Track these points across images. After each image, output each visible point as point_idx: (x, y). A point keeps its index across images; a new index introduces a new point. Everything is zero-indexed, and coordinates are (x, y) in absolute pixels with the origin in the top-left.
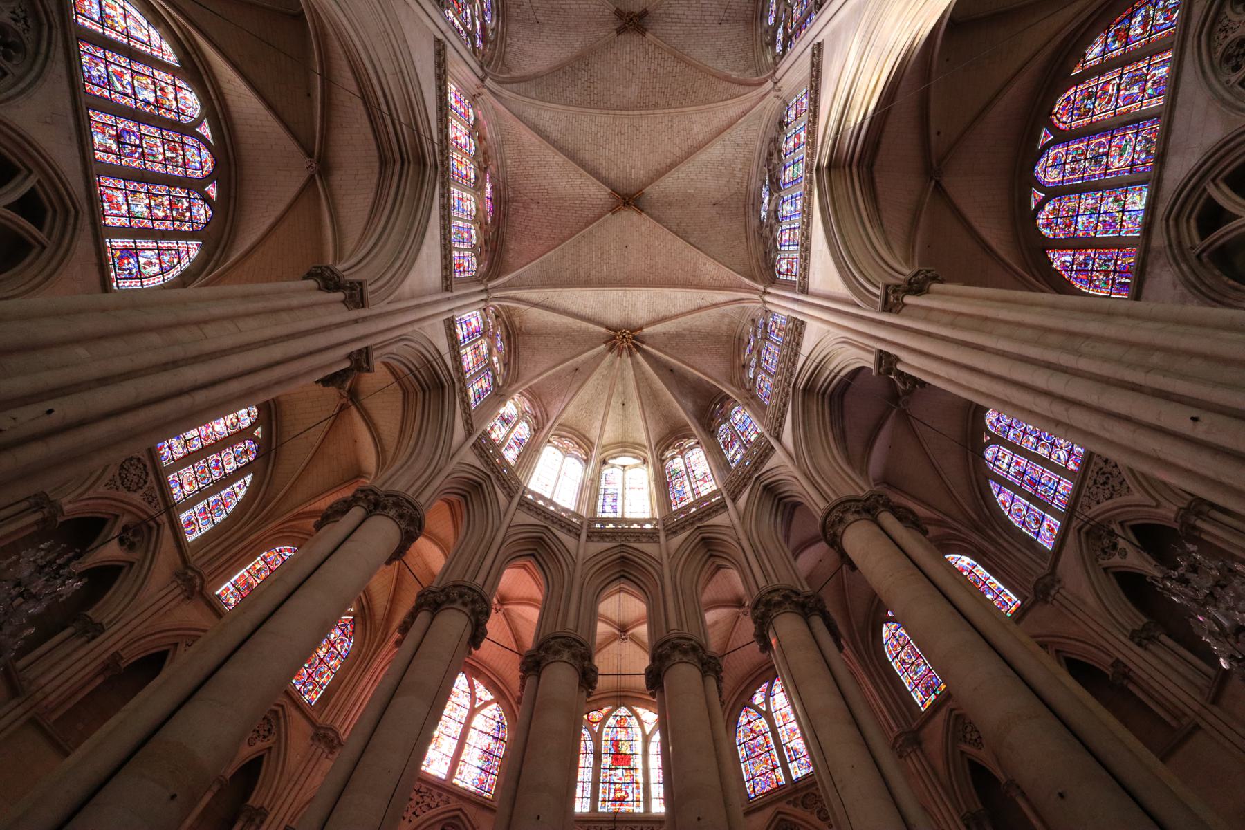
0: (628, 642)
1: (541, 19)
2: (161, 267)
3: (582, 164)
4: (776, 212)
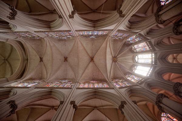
0: (177, 57)
3: (87, 67)
4: (95, 35)
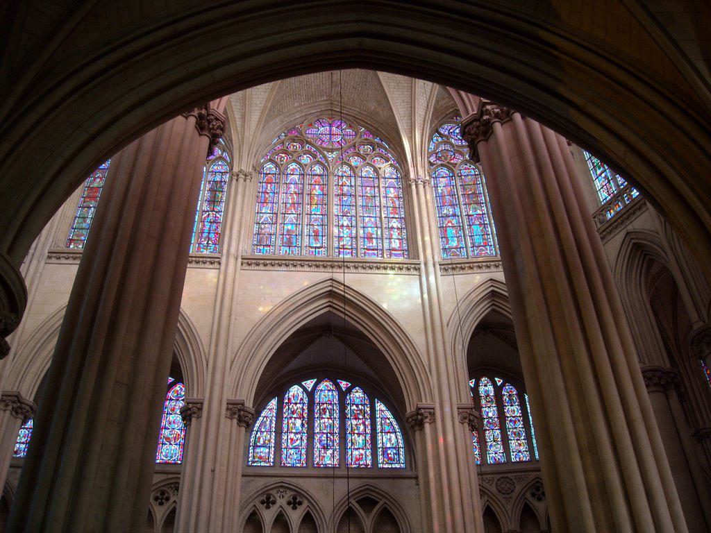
2: (392, 433)
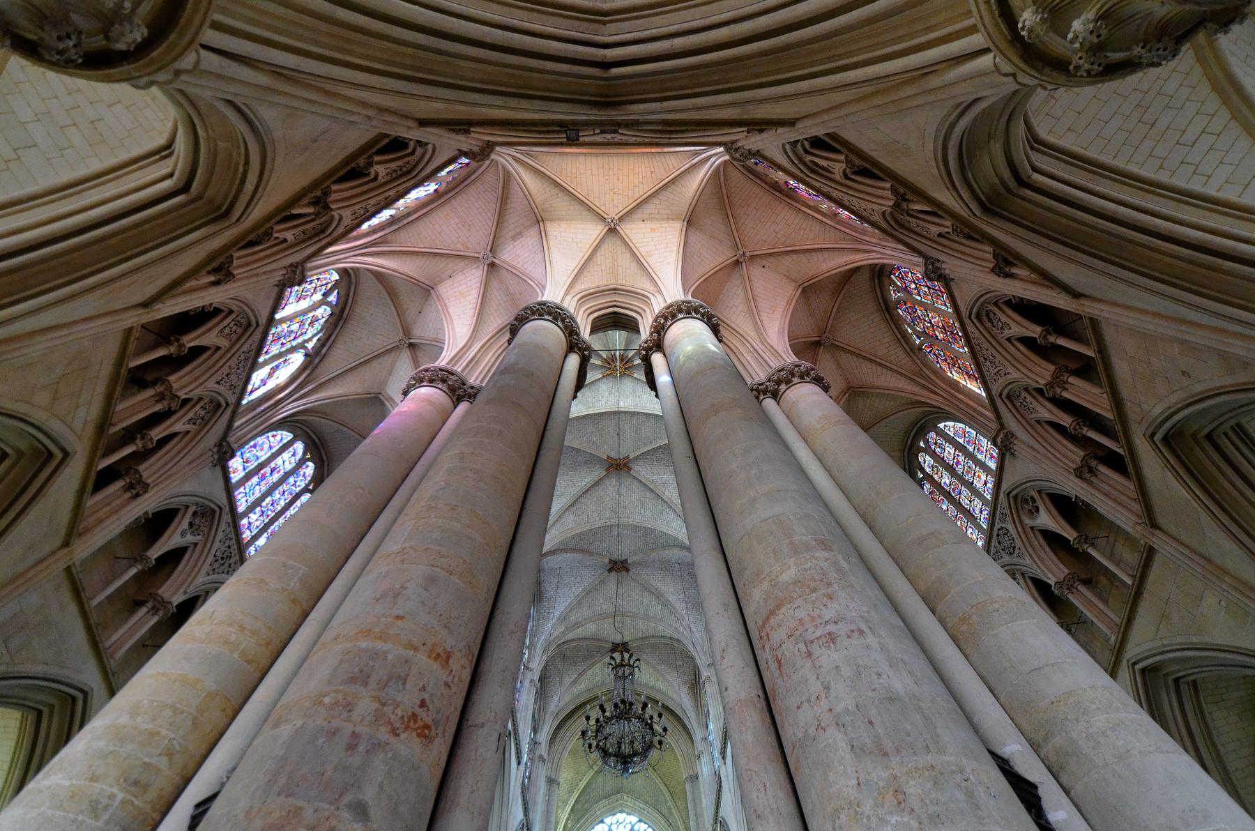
1: (677, 566)
